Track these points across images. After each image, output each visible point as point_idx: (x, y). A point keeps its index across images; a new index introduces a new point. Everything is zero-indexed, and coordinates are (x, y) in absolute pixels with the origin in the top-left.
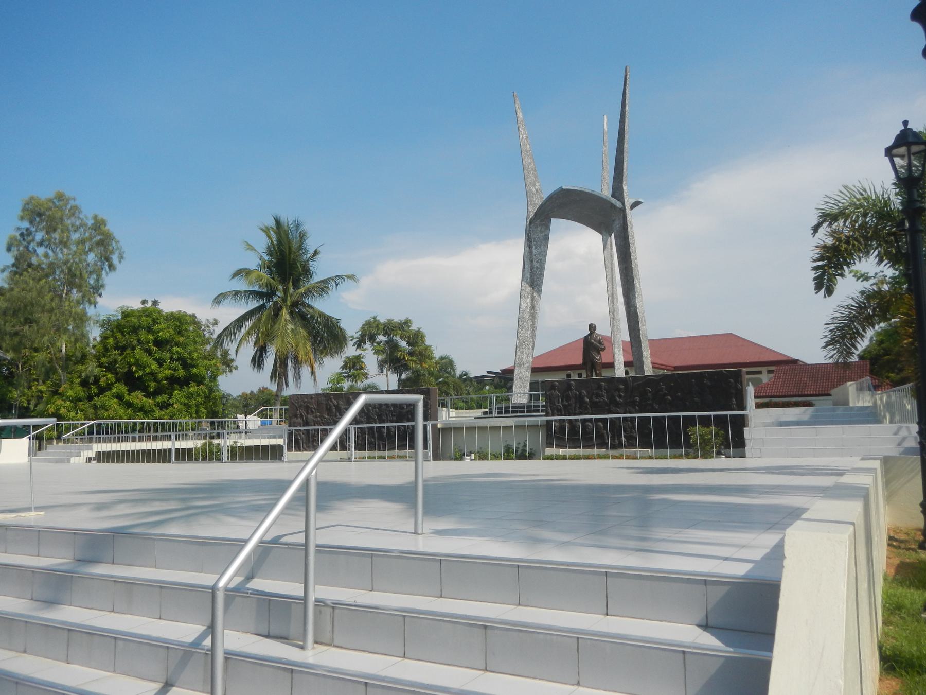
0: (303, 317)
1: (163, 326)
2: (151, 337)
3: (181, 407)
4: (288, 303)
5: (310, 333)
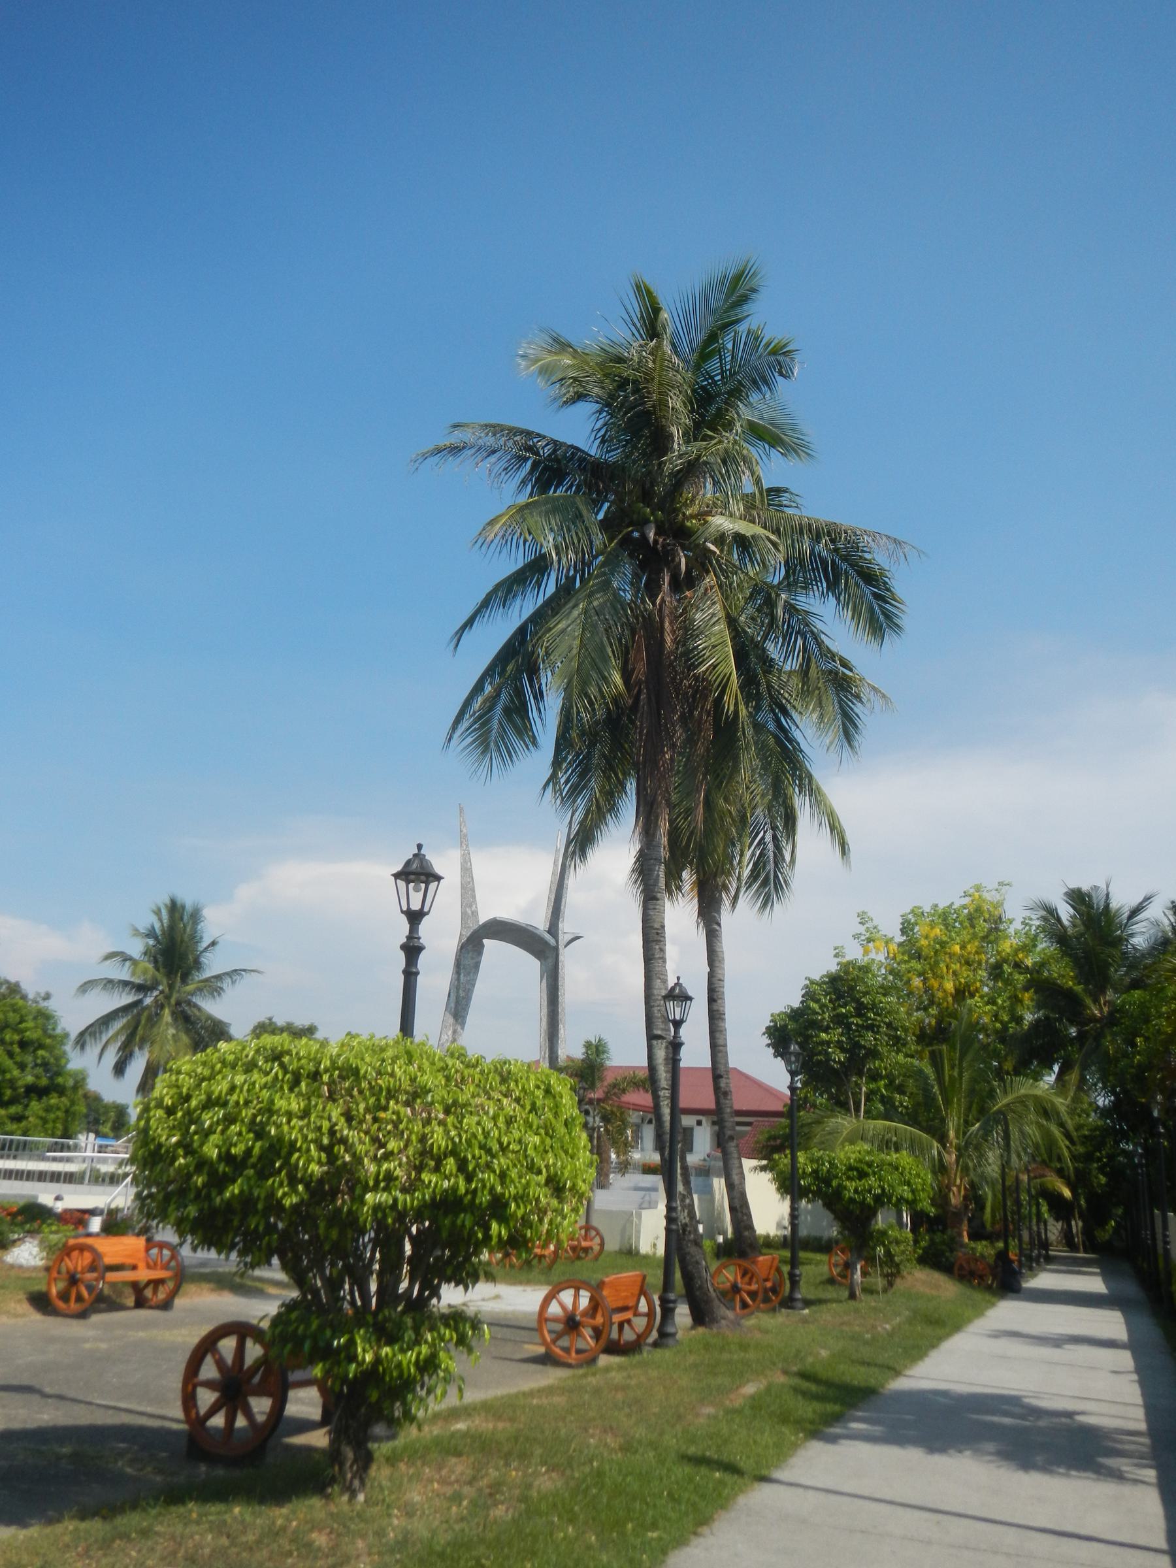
0: (186, 1018)
1: (30, 1024)
2: (16, 1037)
3: (39, 1122)
4: (173, 1001)
5: (192, 1039)
